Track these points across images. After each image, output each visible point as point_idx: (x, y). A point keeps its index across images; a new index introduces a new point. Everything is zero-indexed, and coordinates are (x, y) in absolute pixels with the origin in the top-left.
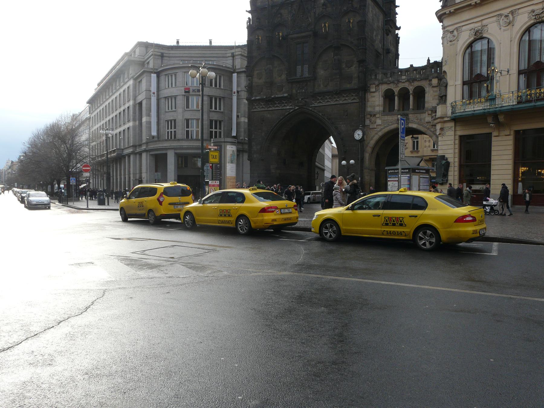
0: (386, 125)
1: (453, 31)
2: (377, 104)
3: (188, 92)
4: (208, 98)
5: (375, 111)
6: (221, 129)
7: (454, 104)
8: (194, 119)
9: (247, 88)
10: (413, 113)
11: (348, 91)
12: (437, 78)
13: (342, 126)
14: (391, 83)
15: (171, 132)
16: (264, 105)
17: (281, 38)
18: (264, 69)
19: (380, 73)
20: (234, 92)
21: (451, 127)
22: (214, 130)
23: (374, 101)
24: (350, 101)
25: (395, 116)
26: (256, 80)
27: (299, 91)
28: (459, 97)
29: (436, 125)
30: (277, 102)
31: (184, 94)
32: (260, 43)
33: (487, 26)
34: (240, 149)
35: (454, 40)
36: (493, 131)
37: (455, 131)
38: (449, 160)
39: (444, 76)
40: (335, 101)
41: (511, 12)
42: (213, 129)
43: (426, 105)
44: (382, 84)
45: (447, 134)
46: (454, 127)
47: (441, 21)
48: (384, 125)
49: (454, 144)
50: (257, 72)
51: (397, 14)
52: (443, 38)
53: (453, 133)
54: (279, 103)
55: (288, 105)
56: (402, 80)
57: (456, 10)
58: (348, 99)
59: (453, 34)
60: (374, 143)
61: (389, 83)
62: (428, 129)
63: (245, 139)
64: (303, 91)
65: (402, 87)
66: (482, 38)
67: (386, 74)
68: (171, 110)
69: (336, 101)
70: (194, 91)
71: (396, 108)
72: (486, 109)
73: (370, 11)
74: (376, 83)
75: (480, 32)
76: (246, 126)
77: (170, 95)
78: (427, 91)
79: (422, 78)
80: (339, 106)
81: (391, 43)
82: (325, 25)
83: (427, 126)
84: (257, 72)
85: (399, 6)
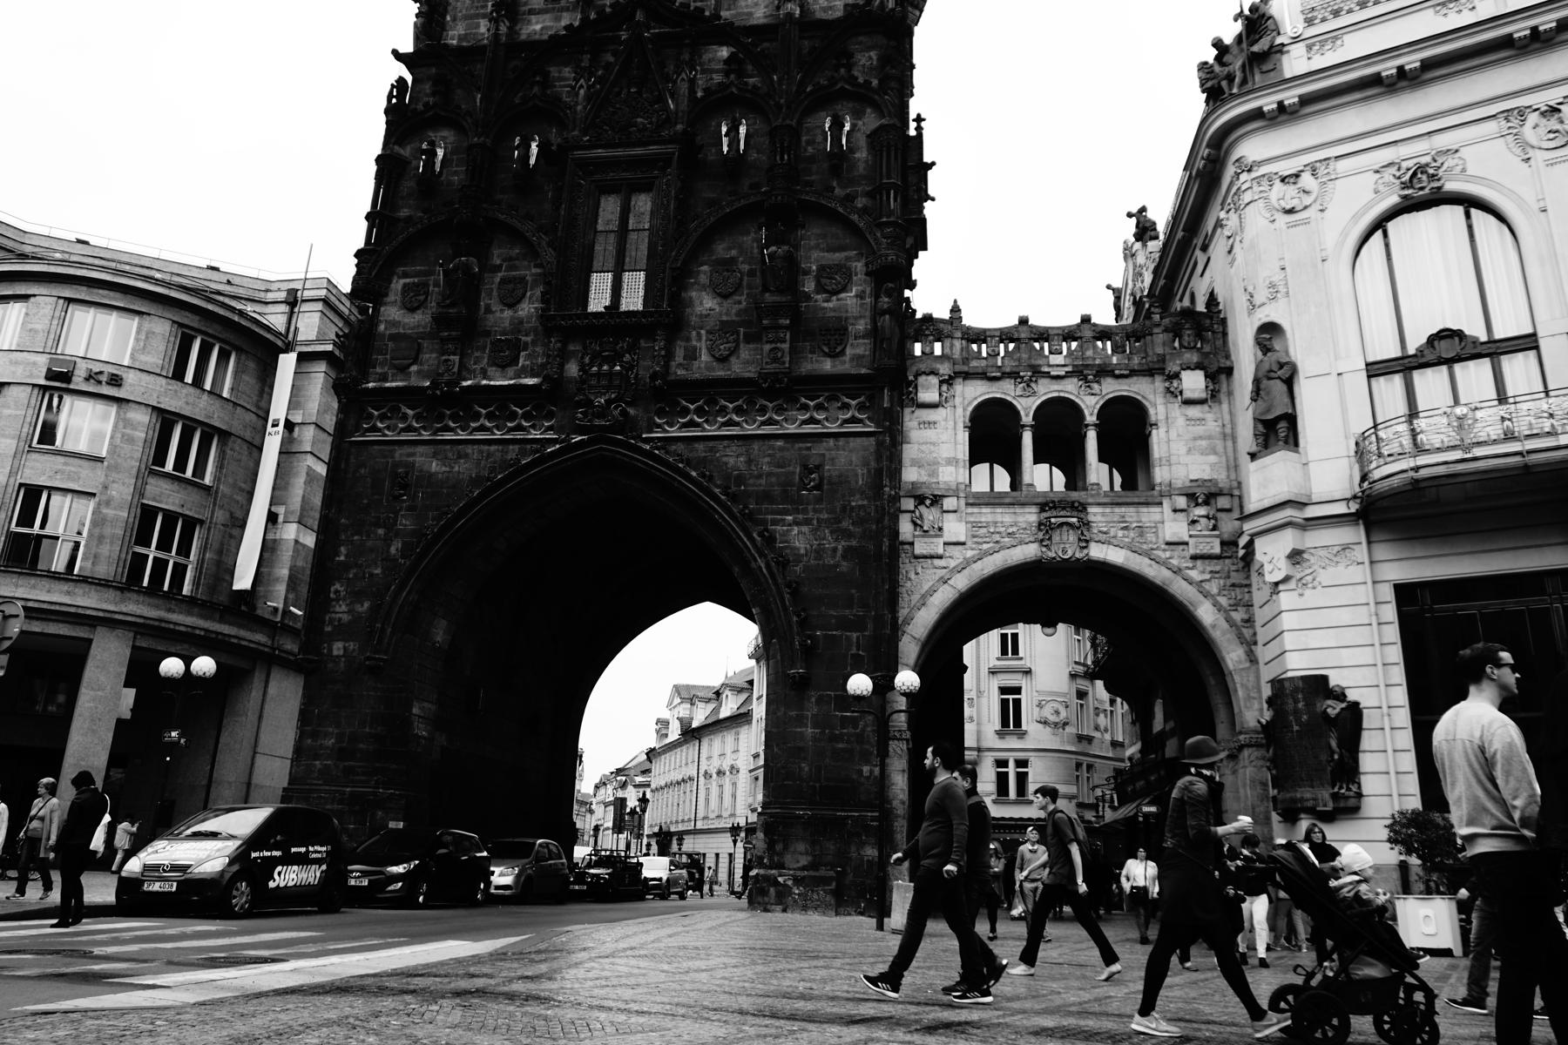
0: (985, 546)
1: (1297, 176)
2: (944, 456)
12: (1201, 369)
14: (1006, 375)
16: (418, 417)
17: (532, 161)
19: (959, 334)
21: (1346, 547)
22: (152, 553)
23: (933, 444)
24: (833, 428)
25: (1027, 510)
26: (393, 312)
27: (595, 369)
30: (484, 411)
31: (43, 382)
34: (261, 648)
35: (1306, 208)
38: (1352, 695)
40: (763, 423)
43: (1160, 475)
44: (964, 379)
45: (1325, 577)
46: (1361, 553)
48: (981, 544)
50: (402, 281)
53: (1361, 573)
54: (490, 417)
55: (533, 427)
57: (1306, 100)
58: (827, 419)
61: (999, 374)
62: (1177, 571)
63: (286, 612)
65: (1050, 396)
69: (770, 422)
70: (91, 377)
74: (941, 372)
75: (1431, 171)
76: (305, 563)
78: (1161, 417)
79: (1136, 368)
80: (780, 443)
82: (733, 130)
83: (1170, 558)
84: (408, 280)
85: (933, 199)
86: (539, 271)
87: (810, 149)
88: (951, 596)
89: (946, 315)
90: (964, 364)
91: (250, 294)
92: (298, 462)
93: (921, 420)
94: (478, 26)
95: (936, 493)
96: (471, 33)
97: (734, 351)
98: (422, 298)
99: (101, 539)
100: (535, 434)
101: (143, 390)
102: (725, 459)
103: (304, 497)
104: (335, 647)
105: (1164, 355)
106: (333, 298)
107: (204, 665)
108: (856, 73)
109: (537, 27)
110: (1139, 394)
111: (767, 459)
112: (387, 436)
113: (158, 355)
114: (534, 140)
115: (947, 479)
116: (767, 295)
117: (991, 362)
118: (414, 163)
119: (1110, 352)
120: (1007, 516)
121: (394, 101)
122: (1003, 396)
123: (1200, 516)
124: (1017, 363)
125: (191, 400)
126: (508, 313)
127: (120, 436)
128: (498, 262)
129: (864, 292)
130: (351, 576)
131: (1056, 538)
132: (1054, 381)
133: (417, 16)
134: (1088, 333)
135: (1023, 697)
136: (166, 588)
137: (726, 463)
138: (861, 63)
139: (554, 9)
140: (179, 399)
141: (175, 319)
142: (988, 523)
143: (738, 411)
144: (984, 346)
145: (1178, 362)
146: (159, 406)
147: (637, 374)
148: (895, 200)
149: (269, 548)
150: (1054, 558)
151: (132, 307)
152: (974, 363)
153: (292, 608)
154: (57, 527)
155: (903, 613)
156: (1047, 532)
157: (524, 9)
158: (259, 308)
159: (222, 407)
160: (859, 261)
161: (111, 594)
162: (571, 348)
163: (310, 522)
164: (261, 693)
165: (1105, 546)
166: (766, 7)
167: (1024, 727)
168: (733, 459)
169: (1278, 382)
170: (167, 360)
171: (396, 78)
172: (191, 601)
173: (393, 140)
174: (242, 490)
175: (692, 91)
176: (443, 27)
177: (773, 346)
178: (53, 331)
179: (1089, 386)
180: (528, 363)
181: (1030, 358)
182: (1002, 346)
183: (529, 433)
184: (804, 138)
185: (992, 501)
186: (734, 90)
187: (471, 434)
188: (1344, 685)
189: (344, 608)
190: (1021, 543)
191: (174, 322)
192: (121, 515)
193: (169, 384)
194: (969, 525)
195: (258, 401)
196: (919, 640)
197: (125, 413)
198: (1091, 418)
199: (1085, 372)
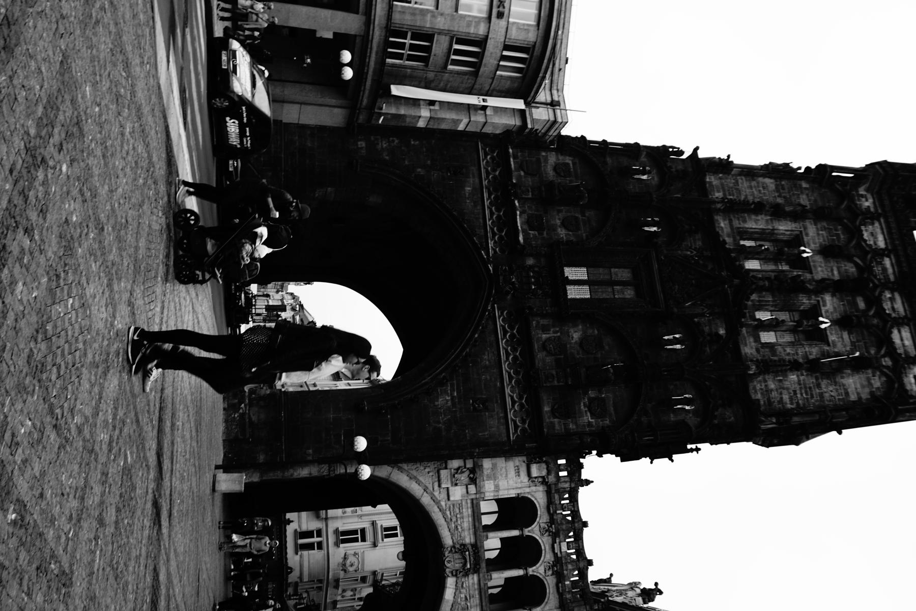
0: (448, 513)
2: (500, 483)
4: (481, 37)
6: (408, 60)
11: (532, 411)
13: (448, 398)
14: (551, 516)
16: (495, 177)
17: (646, 229)
19: (573, 485)
22: (408, 41)
23: (506, 476)
24: (510, 415)
25: (472, 537)
26: (552, 159)
27: (532, 274)
30: (501, 214)
32: (636, 177)
34: (359, 102)
40: (509, 374)
42: (412, 39)
44: (546, 491)
48: (450, 510)
50: (570, 162)
54: (499, 217)
55: (495, 242)
56: (558, 543)
58: (515, 411)
60: (401, 484)
61: (552, 512)
63: (380, 115)
65: (542, 544)
69: (510, 378)
74: (550, 477)
82: (676, 341)
84: (571, 165)
85: (651, 463)
86: (584, 238)
87: (672, 387)
88: (417, 494)
89: (583, 477)
90: (555, 490)
93: (520, 467)
94: (718, 192)
95: (478, 480)
97: (549, 353)
98: (562, 174)
99: (413, 14)
100: (491, 244)
101: (497, 30)
103: (445, 119)
104: (362, 142)
106: (557, 125)
107: (348, 73)
108: (720, 410)
109: (723, 224)
111: (488, 377)
112: (483, 162)
113: (515, 36)
114: (658, 229)
116: (584, 369)
117: (559, 506)
118: (637, 163)
119: (572, 579)
120: (468, 524)
121: (671, 150)
122: (539, 516)
124: (559, 522)
125: (494, 55)
126: (558, 222)
127: (471, 19)
128: (587, 215)
129: (592, 426)
130: (403, 148)
131: (457, 556)
132: (551, 546)
133: (719, 158)
134: (582, 565)
135: (360, 543)
136: (390, 50)
137: (484, 354)
138: (726, 413)
139: (734, 233)
140: (493, 48)
141: (537, 44)
142: (462, 513)
143: (515, 358)
144: (568, 501)
146: (489, 40)
147: (531, 298)
148: (648, 440)
149: (415, 102)
150: (445, 556)
151: (541, 20)
152: (557, 496)
153: (382, 117)
155: (405, 466)
156: (460, 550)
158: (548, 87)
161: (384, 22)
162: (542, 260)
163: (430, 122)
164: (334, 104)
165: (454, 587)
166: (751, 354)
167: (341, 545)
168: (487, 358)
170: (515, 41)
171: (684, 150)
172: (381, 63)
174: (446, 85)
175: (697, 316)
176: (715, 173)
177: (555, 376)
179: (550, 568)
180: (531, 236)
181: (563, 530)
182: (569, 512)
185: (476, 515)
186: (701, 340)
187: (488, 207)
189: (385, 145)
190: (452, 535)
191: (535, 43)
192: (427, 23)
194: (460, 502)
196: (389, 477)
198: (531, 571)
199: (558, 564)
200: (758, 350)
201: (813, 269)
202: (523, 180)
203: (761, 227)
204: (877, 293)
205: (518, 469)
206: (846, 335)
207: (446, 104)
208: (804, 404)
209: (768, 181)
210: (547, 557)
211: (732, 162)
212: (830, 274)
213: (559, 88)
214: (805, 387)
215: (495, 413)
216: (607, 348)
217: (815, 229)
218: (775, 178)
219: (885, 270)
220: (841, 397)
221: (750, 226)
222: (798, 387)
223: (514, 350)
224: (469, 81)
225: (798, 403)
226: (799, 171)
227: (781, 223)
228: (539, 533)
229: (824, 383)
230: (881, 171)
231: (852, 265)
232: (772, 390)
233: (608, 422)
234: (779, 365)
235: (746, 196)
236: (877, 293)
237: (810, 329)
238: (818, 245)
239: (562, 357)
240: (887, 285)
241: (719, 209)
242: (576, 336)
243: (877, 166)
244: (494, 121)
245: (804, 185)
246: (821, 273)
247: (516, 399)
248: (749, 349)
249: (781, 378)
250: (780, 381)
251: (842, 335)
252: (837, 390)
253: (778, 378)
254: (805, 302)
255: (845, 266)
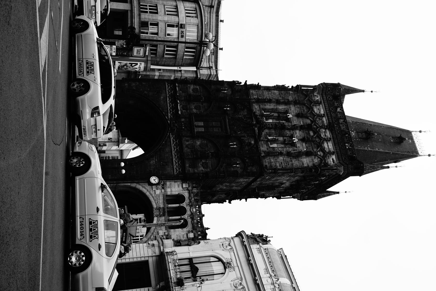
0: (155, 198)
2: (173, 189)
3: (181, 27)
5: (167, 188)
7: (175, 254)
8: (158, 31)
9: (186, 79)
10: (166, 220)
11: (182, 166)
13: (154, 161)
14: (190, 200)
15: (147, 9)
16: (171, 94)
17: (225, 109)
18: (201, 94)
19: (198, 191)
20: (181, 68)
21: (155, 253)
23: (175, 187)
24: (175, 167)
25: (163, 205)
26: (192, 87)
27: (183, 124)
28: (180, 256)
29: (156, 240)
30: (173, 105)
31: (180, 23)
33: (233, 271)
35: (223, 247)
36: (152, 288)
37: (152, 256)
38: (127, 254)
39: (196, 242)
40: (175, 154)
41: (244, 287)
44: (189, 193)
45: (150, 250)
46: (155, 255)
47: (237, 236)
48: (155, 197)
49: (141, 257)
50: (199, 88)
51: (240, 200)
52: (225, 238)
53: (150, 255)
54: (172, 106)
55: (171, 114)
57: (245, 246)
58: (177, 166)
59: (228, 246)
62: (153, 234)
63: (139, 75)
64: (183, 128)
66: (225, 268)
67: (196, 195)
68: (166, 10)
69: (175, 156)
70: (182, 32)
71: (170, 205)
72: (171, 280)
73: (244, 180)
74: (189, 188)
75: (230, 266)
77: (179, 10)
81: (219, 197)
82: (234, 145)
85: (246, 201)
86: (203, 112)
87: (233, 160)
90: (192, 192)
91: (211, 59)
92: (173, 73)
96: (253, 95)
97: (189, 148)
98: (195, 92)
100: (169, 115)
102: (167, 148)
103: (165, 75)
104: (126, 84)
105: (197, 230)
106: (212, 76)
110: (188, 226)
111: (168, 155)
112: (167, 89)
115: (168, 190)
116: (200, 153)
122: (186, 200)
123: (164, 237)
125: (181, 51)
126: (193, 107)
129: (203, 171)
130: (140, 85)
131: (158, 211)
134: (200, 216)
137: (167, 148)
139: (261, 110)
143: (177, 150)
145: (195, 232)
146: (179, 46)
149: (154, 70)
151: (199, 37)
153: (140, 76)
154: (150, 30)
156: (158, 209)
157: (260, 104)
159: (181, 57)
160: (210, 170)
162: (187, 119)
168: (167, 150)
169: (188, 243)
173: (227, 83)
176: (254, 89)
178: (191, 23)
180: (184, 112)
181: (194, 205)
183: (169, 114)
184: (235, 158)
186: (243, 144)
188: (129, 253)
190: (156, 204)
193: (184, 46)
194: (159, 195)
195: (185, 64)
197: (176, 39)
200: (267, 149)
201: (292, 122)
202: (181, 94)
203: (272, 107)
204: (318, 130)
205: (179, 185)
206: (304, 144)
207: (165, 70)
208: (285, 167)
209: (275, 91)
210: (188, 213)
211: (260, 85)
212: (299, 123)
213: (212, 61)
214: (286, 162)
215: (170, 166)
216: (209, 147)
217: (294, 108)
218: (278, 90)
219: (323, 122)
220: (300, 165)
221: (267, 107)
222: (283, 161)
223: (177, 147)
224: (174, 61)
225: (282, 167)
226: (288, 88)
227: (280, 106)
228: (186, 205)
229: (293, 161)
230: (322, 86)
231: (309, 120)
232: (272, 162)
233: (209, 170)
234: (273, 153)
235: (266, 97)
236: (318, 130)
237: (291, 142)
238: (295, 113)
239: (193, 149)
240: (323, 127)
241: (254, 102)
242: (198, 143)
243: (320, 85)
244: (185, 76)
245: (291, 92)
246: (295, 123)
247: (177, 162)
248: (263, 148)
249: (276, 158)
250: (276, 159)
251: (303, 144)
252: (299, 163)
253: (275, 158)
254: (288, 133)
255: (306, 120)
